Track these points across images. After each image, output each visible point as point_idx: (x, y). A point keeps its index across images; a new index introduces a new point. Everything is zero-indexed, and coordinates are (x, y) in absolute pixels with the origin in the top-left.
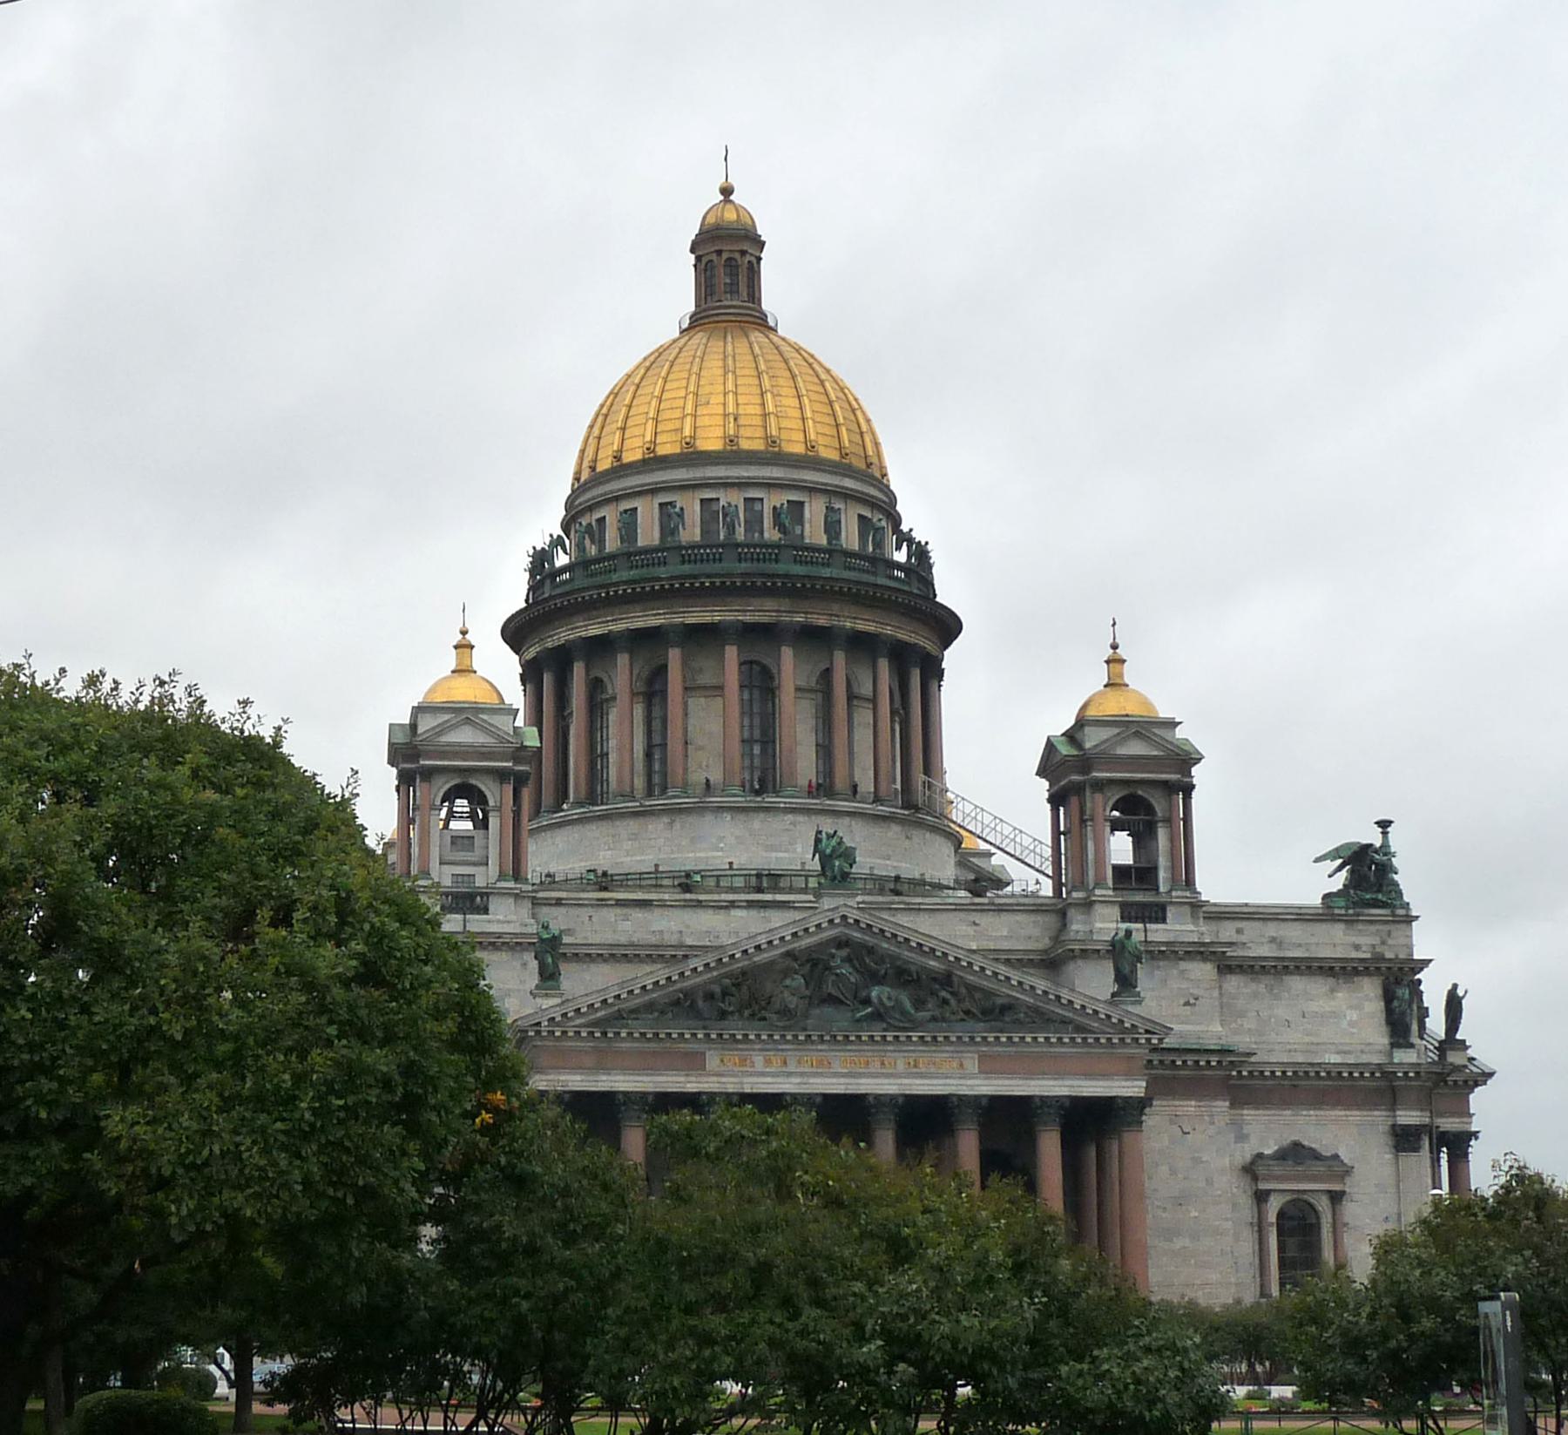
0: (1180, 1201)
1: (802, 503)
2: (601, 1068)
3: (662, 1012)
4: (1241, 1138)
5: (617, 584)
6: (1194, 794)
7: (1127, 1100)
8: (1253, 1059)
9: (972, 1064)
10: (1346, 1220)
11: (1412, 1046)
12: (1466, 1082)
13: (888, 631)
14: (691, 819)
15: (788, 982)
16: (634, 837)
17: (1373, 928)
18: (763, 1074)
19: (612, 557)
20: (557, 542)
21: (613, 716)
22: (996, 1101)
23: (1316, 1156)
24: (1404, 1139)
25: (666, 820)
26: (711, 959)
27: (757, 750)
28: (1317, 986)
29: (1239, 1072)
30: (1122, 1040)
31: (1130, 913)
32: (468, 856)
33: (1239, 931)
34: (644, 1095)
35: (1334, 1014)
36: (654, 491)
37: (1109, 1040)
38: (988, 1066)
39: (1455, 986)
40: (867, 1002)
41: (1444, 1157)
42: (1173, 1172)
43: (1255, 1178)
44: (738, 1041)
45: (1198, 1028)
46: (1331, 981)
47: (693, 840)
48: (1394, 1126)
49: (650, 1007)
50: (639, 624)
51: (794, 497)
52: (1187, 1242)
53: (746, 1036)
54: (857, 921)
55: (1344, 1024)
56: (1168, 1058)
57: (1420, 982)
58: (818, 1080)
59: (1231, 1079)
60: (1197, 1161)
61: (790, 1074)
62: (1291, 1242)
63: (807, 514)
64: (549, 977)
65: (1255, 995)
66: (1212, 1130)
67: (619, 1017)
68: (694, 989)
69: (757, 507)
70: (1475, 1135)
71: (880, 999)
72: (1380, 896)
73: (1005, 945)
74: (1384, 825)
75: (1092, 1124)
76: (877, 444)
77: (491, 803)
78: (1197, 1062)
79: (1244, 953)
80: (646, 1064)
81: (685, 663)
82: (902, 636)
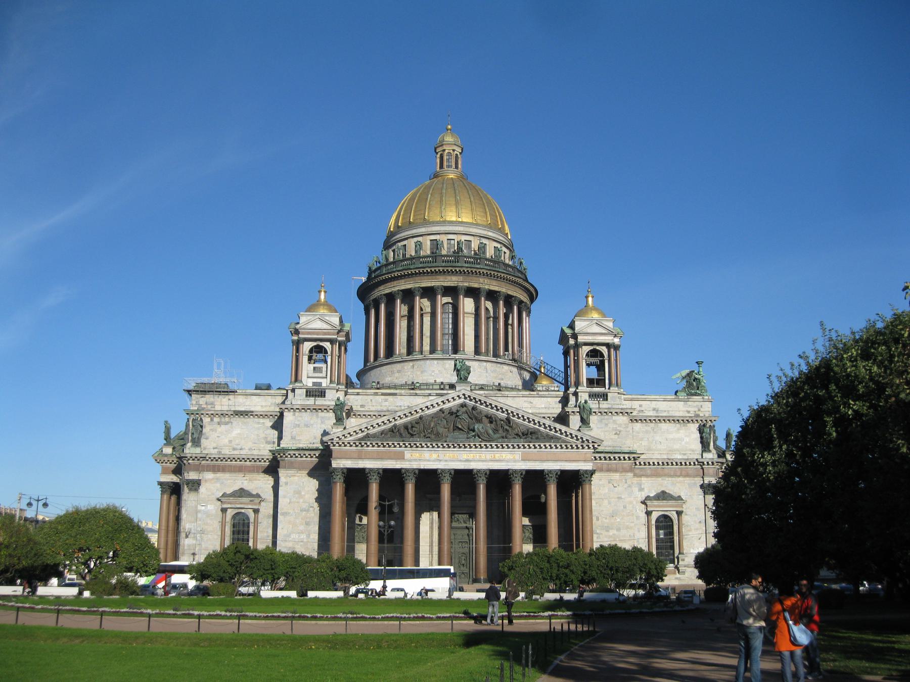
2: (360, 458)
3: (386, 434)
8: (642, 457)
11: (710, 451)
13: (504, 290)
14: (422, 362)
16: (399, 372)
18: (429, 461)
25: (411, 364)
26: (406, 412)
31: (592, 396)
32: (320, 375)
33: (640, 406)
34: (378, 469)
35: (682, 440)
40: (474, 431)
42: (610, 503)
47: (422, 372)
49: (382, 433)
50: (403, 288)
51: (468, 238)
52: (615, 532)
56: (607, 456)
59: (631, 462)
62: (661, 532)
64: (339, 420)
65: (647, 432)
66: (626, 485)
67: (367, 437)
69: (452, 242)
73: (544, 411)
80: (380, 457)
82: (510, 293)
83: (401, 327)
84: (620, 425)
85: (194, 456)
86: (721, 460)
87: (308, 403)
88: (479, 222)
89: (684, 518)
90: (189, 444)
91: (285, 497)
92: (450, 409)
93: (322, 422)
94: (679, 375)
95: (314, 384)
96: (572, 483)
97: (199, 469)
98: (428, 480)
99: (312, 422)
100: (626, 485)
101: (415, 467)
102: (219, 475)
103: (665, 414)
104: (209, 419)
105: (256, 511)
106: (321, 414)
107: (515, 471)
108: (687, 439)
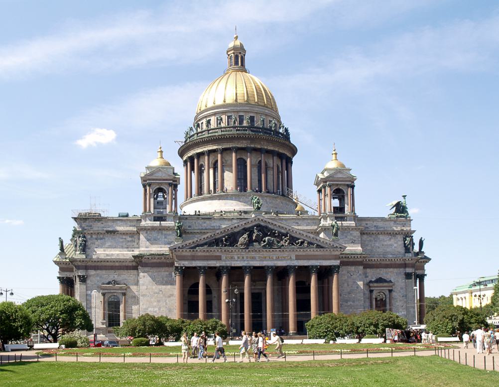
0: (349, 293)
1: (254, 117)
4: (366, 277)
5: (204, 138)
6: (355, 188)
7: (335, 266)
9: (294, 258)
10: (393, 296)
12: (424, 262)
13: (277, 150)
15: (243, 236)
16: (210, 204)
17: (401, 223)
19: (204, 131)
20: (191, 129)
21: (205, 174)
22: (300, 267)
23: (385, 281)
24: (408, 276)
27: (242, 181)
28: (386, 238)
29: (366, 260)
30: (333, 250)
31: (337, 218)
35: (391, 245)
36: (214, 114)
37: (330, 250)
38: (298, 258)
39: (422, 238)
40: (264, 241)
41: (418, 281)
42: (348, 285)
43: (370, 287)
44: (230, 252)
45: (356, 248)
46: (390, 237)
48: (405, 273)
51: (252, 115)
52: (351, 303)
53: (232, 251)
54: (262, 220)
55: (393, 247)
57: (412, 236)
58: (252, 262)
60: (355, 282)
61: (245, 261)
63: (255, 119)
65: (370, 241)
68: (218, 239)
69: (242, 117)
70: (426, 275)
71: (268, 240)
72: (403, 214)
74: (404, 196)
75: (325, 274)
76: (275, 102)
77: (167, 192)
78: (354, 257)
79: (368, 229)
81: (222, 158)
82: (281, 151)
83: (208, 175)
84: (355, 237)
85: (82, 260)
86: (416, 258)
87: (155, 225)
88: (260, 103)
89: (394, 294)
90: (78, 253)
91: (143, 285)
92: (250, 228)
93: (165, 238)
94: (390, 204)
95: (158, 213)
96: (325, 274)
97: (86, 268)
98: (236, 274)
99: (159, 237)
100: (358, 275)
101: (228, 265)
102: (99, 272)
103: (382, 229)
104: (89, 237)
105: (124, 294)
106: (164, 232)
107: (290, 267)
108: (396, 245)
